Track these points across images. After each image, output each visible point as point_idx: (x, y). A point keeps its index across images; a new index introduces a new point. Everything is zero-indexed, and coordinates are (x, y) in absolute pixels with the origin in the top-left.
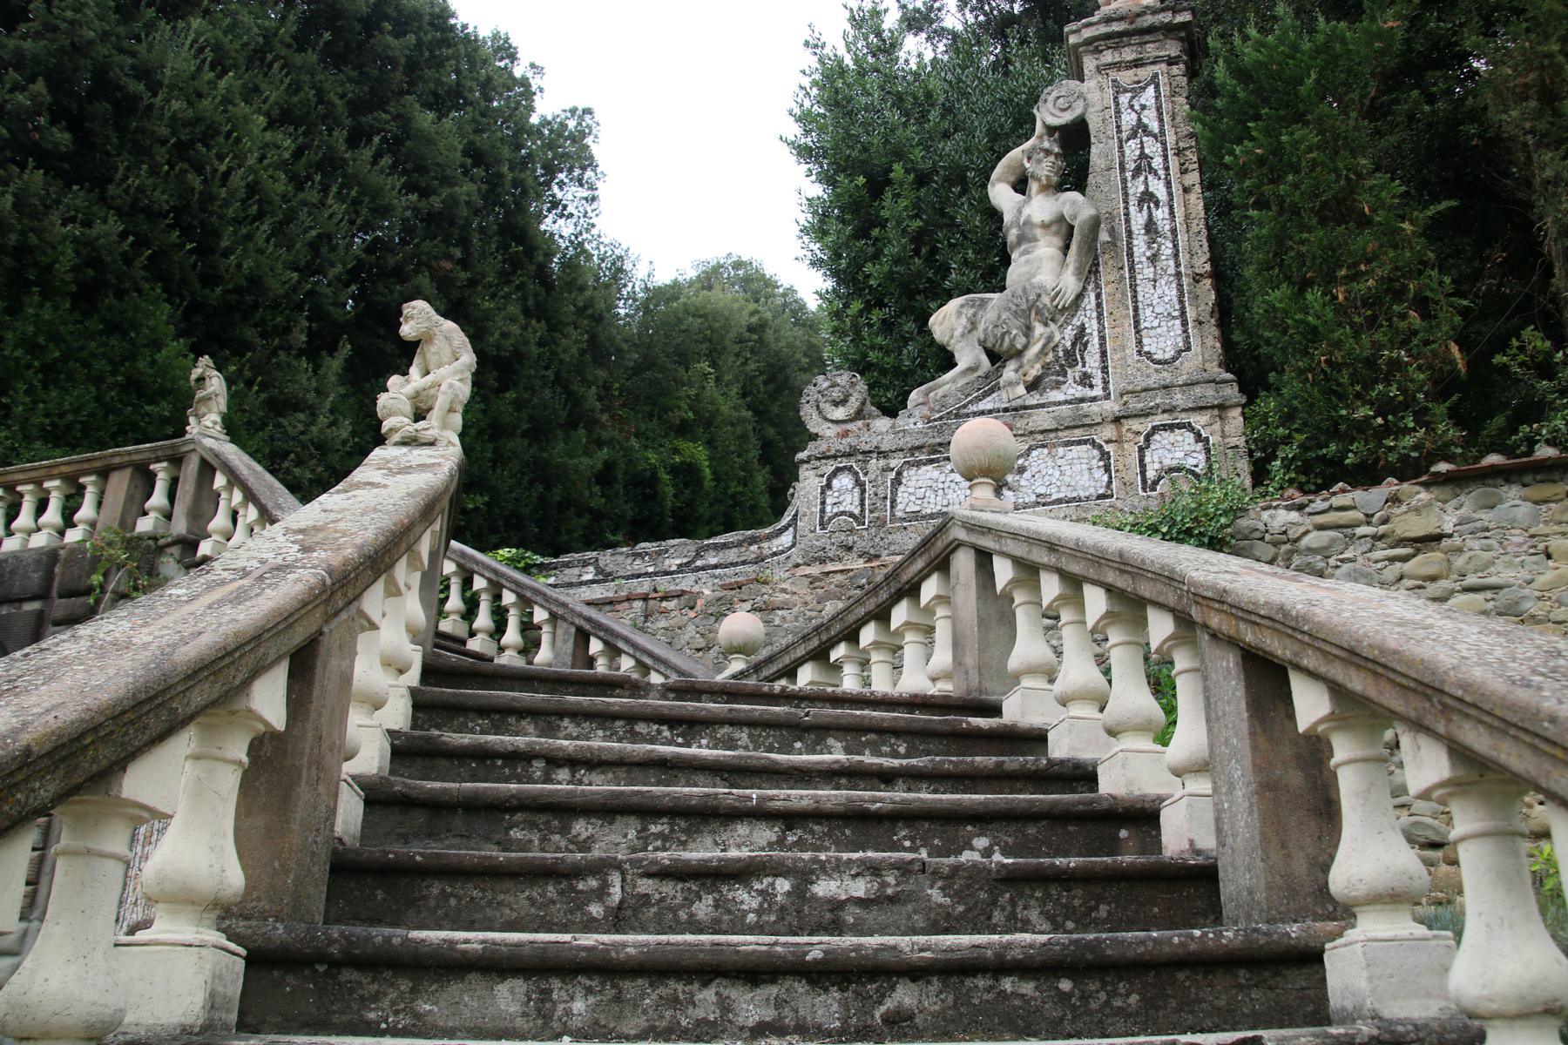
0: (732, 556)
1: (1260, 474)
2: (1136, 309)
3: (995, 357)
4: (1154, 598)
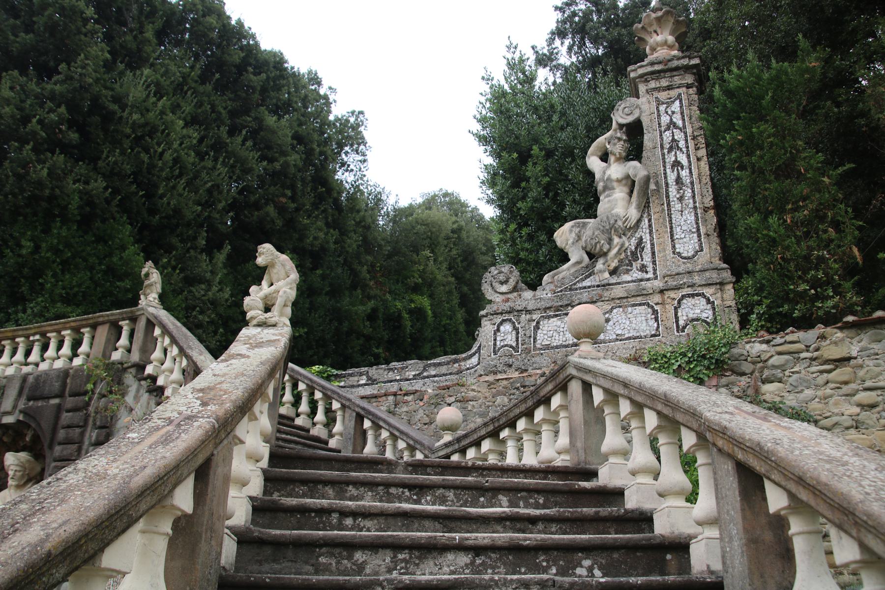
0: (443, 369)
1: (744, 322)
2: (671, 228)
3: (591, 256)
4: (684, 423)
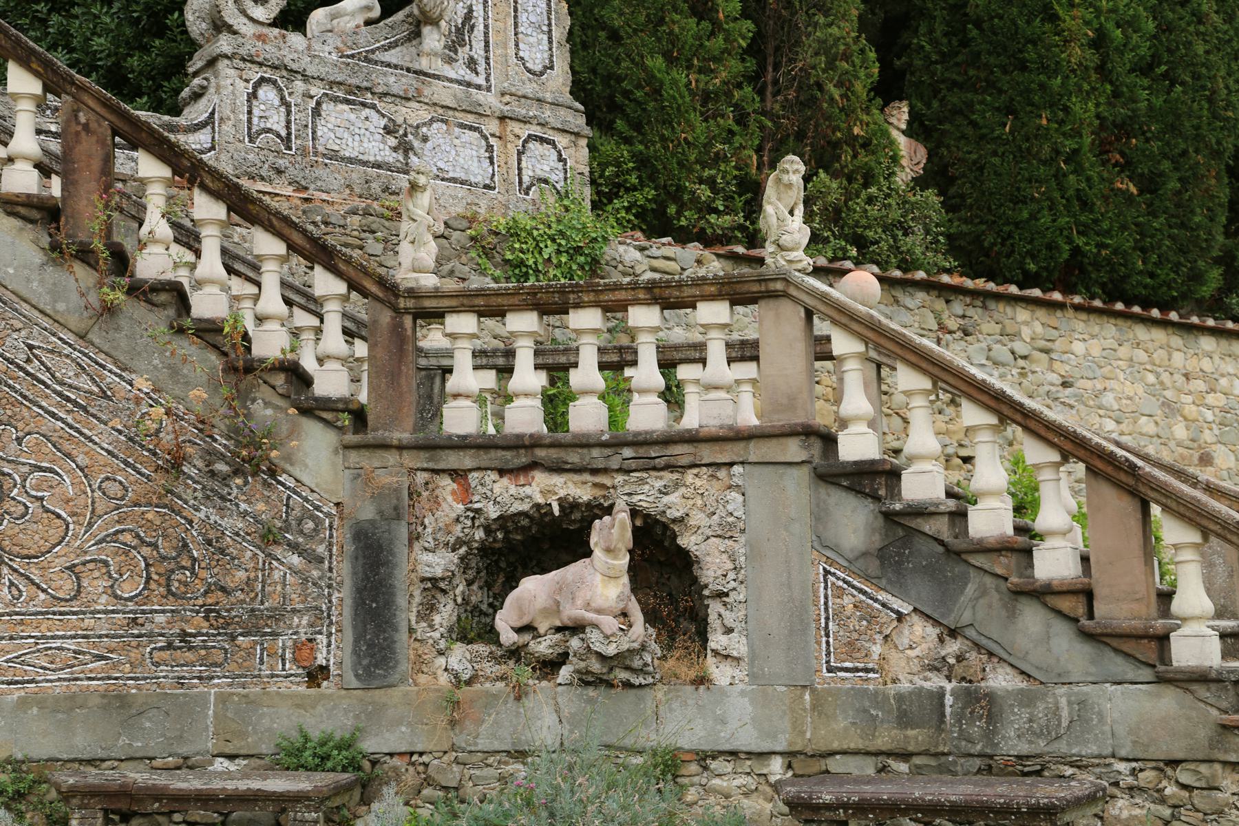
2: (516, 10)
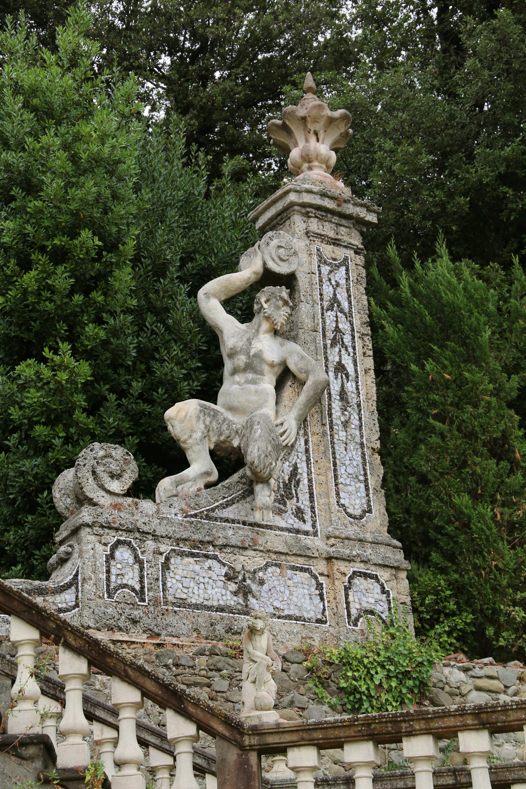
2: (335, 465)
